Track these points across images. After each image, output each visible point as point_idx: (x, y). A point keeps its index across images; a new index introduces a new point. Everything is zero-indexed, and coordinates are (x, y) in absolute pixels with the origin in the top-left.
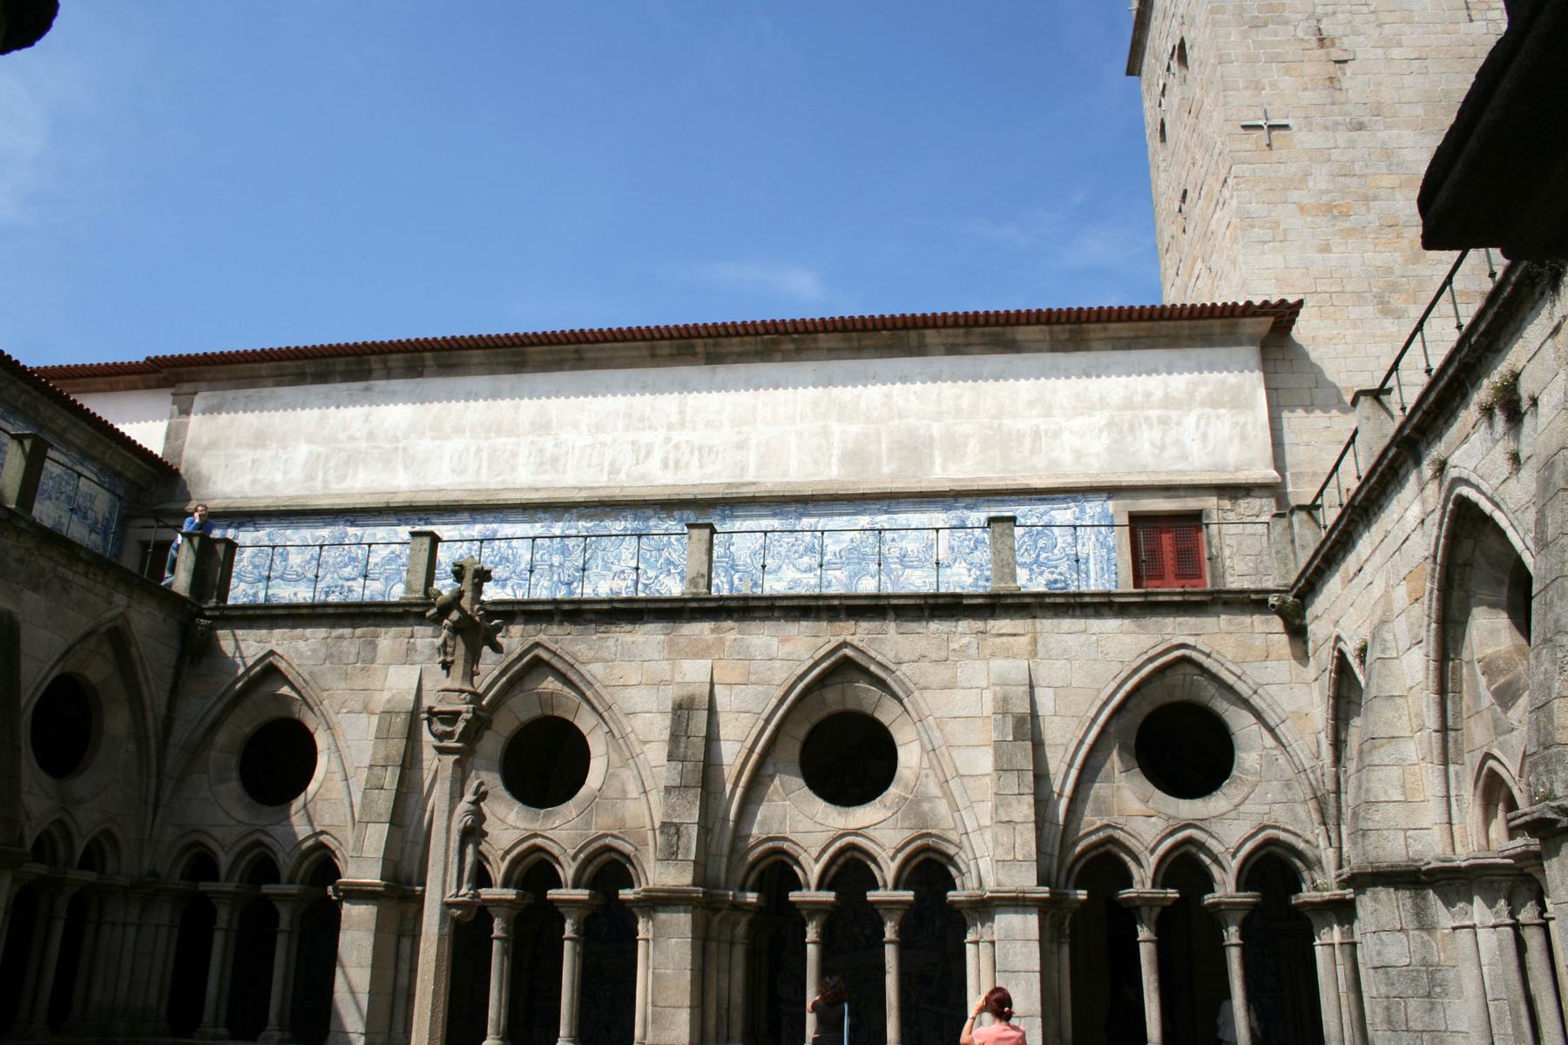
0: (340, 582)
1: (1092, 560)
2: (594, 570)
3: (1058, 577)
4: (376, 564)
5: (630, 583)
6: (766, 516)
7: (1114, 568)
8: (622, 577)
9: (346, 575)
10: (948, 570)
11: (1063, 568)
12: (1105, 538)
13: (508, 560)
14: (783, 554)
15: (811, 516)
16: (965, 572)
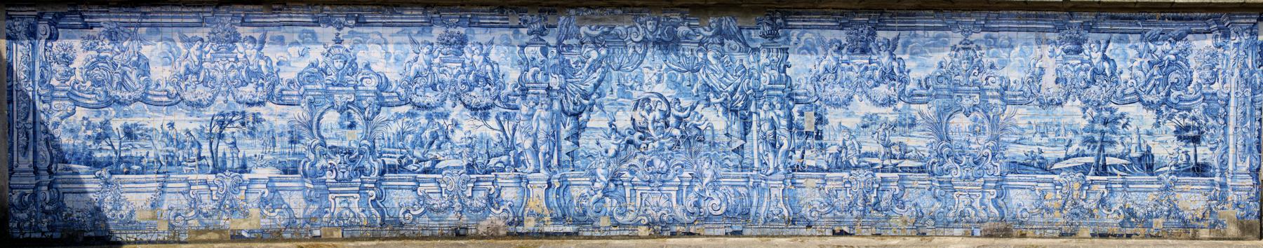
0: (240, 108)
1: (1232, 102)
2: (607, 97)
3: (1191, 123)
4: (291, 82)
5: (658, 115)
6: (830, 28)
7: (1258, 113)
8: (647, 107)
9: (247, 97)
10: (1059, 108)
11: (1198, 111)
12: (1251, 74)
13: (487, 80)
14: (854, 79)
15: (888, 29)
16: (1080, 112)
